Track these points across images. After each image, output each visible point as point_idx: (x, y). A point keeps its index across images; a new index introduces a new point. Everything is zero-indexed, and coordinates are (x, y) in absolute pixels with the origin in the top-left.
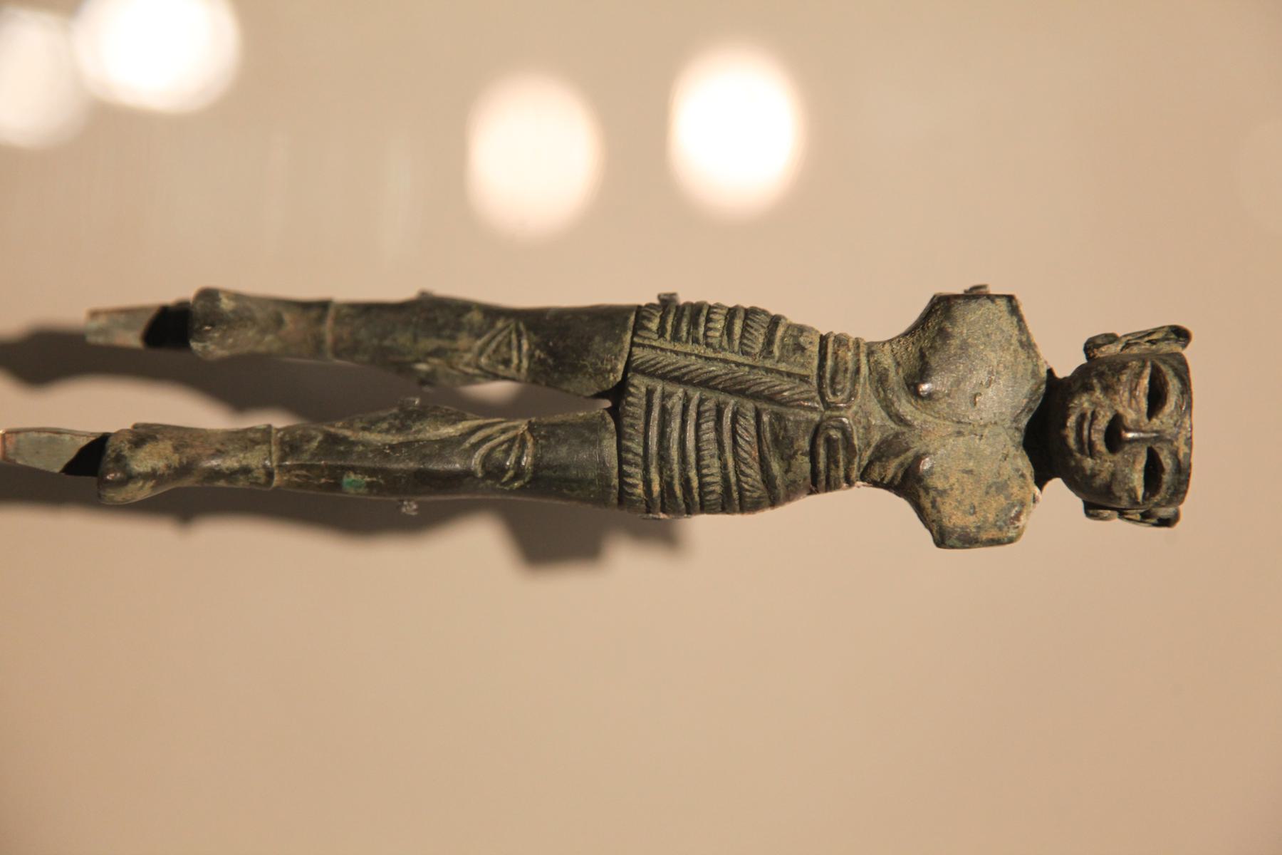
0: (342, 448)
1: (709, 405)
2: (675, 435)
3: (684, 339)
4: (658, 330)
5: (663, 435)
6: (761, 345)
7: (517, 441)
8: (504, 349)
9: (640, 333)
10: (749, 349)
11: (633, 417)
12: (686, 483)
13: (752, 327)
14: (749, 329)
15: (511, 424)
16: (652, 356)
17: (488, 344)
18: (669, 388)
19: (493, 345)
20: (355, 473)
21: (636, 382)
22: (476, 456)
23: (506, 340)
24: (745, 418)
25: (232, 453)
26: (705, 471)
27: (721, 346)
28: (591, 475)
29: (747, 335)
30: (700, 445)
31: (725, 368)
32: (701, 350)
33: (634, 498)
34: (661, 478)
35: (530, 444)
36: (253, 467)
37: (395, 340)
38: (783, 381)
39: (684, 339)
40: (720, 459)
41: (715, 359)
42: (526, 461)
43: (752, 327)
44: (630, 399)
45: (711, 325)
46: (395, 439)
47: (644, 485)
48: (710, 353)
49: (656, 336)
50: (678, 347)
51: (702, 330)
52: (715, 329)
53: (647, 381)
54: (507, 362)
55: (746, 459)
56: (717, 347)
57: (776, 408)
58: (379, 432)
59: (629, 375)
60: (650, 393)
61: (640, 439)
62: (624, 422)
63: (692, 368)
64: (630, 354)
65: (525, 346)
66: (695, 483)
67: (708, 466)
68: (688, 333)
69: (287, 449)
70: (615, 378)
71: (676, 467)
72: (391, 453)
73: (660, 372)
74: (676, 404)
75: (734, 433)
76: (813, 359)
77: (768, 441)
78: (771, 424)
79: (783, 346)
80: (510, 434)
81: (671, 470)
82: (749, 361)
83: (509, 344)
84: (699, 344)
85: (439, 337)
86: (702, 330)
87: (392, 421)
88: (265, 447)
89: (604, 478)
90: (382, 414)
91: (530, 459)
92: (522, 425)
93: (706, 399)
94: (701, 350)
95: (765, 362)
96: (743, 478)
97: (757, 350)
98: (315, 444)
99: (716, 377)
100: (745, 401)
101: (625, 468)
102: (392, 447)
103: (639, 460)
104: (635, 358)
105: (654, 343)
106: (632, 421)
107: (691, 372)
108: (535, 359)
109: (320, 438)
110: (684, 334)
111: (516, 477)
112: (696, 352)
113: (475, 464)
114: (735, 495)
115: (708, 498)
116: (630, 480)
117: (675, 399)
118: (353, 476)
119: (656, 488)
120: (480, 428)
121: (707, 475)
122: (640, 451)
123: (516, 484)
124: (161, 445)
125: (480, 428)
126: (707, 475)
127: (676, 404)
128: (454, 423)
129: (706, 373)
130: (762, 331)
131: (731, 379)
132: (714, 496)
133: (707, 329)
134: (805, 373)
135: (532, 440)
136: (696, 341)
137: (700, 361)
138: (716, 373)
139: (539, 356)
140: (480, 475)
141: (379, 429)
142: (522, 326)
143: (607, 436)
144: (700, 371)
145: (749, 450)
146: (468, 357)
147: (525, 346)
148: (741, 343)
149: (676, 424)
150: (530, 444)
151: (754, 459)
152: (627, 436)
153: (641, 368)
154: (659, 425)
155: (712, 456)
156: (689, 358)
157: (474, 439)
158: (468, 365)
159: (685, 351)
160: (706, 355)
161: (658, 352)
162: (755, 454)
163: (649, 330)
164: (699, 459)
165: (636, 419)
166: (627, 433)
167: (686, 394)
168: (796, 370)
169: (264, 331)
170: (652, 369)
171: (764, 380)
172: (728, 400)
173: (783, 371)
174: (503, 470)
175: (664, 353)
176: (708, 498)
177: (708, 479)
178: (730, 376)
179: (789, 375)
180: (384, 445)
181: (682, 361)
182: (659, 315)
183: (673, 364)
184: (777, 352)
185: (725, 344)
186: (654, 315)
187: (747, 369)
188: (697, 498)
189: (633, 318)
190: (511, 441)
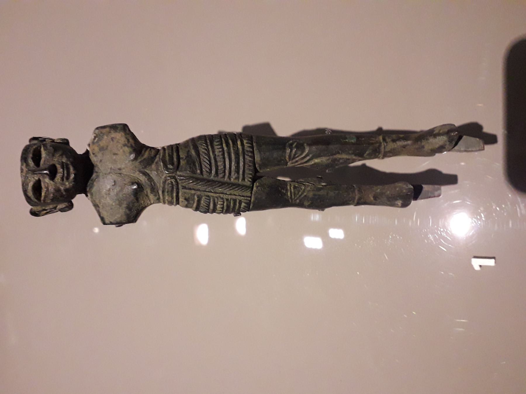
0: (357, 151)
1: (221, 176)
2: (233, 163)
3: (232, 200)
4: (242, 203)
5: (238, 163)
6: (202, 199)
7: (292, 158)
8: (296, 192)
9: (248, 201)
10: (207, 198)
11: (249, 170)
12: (228, 145)
13: (206, 206)
14: (207, 205)
15: (293, 165)
16: (244, 193)
17: (302, 194)
18: (236, 181)
19: (300, 193)
20: (352, 142)
21: (249, 183)
22: (307, 151)
23: (296, 195)
24: (207, 171)
25: (399, 147)
26: (221, 150)
27: (218, 199)
28: (264, 146)
29: (208, 203)
30: (223, 160)
31: (216, 190)
32: (225, 197)
33: (247, 139)
34: (237, 147)
35: (287, 157)
36: (391, 142)
37: (334, 193)
38: (192, 186)
39: (232, 200)
40: (215, 155)
41: (219, 193)
42: (288, 151)
43: (206, 206)
44: (251, 176)
45: (222, 206)
46: (338, 156)
47: (244, 143)
48: (222, 195)
49: (242, 200)
50: (234, 197)
51: (225, 204)
52: (219, 204)
53: (245, 183)
54: (295, 187)
55: (205, 155)
56: (219, 198)
57: (195, 176)
58: (343, 158)
59: (251, 185)
60: (244, 179)
61: (247, 161)
62: (253, 167)
63: (228, 190)
64: (251, 193)
65: (289, 193)
66: (224, 145)
67: (220, 152)
68: (230, 203)
69: (378, 150)
70: (256, 184)
71: (232, 151)
72: (339, 150)
73: (240, 187)
74: (234, 175)
75: (210, 165)
76: (181, 195)
77: (197, 162)
78: (196, 169)
79: (193, 200)
80: (294, 161)
81: (234, 150)
82: (206, 193)
83: (295, 194)
84: (226, 199)
85: (319, 195)
86: (225, 204)
87: (338, 163)
88: (387, 150)
89: (259, 145)
90: (342, 166)
91: (287, 152)
92: (290, 164)
93: (222, 178)
94: (225, 197)
95: (200, 194)
96: (206, 148)
97: (204, 198)
98: (367, 152)
99: (219, 186)
100: (207, 178)
101: (251, 150)
102: (339, 153)
103: (246, 153)
104: (249, 192)
105: (243, 198)
106: (249, 168)
107: (228, 188)
108: (285, 189)
109: (365, 155)
110: (232, 202)
111: (291, 145)
112: (227, 196)
113: (307, 148)
114: (208, 141)
115: (219, 140)
116: (249, 145)
117: (234, 177)
118: (353, 141)
119: (239, 143)
120: (306, 162)
121: (220, 148)
122: (246, 157)
123: (291, 142)
124: (430, 148)
125: (306, 162)
126: (220, 148)
127: (234, 175)
128: (315, 164)
129: (223, 188)
130: (202, 205)
131: (213, 186)
132: (216, 140)
133: (223, 204)
134: (184, 190)
135: (286, 159)
136: (227, 200)
137: (225, 192)
138: (219, 188)
139: (284, 190)
140: (305, 144)
141: (343, 160)
142: (290, 200)
143: (259, 162)
144: (225, 188)
145: (204, 158)
146: (309, 189)
147: (289, 193)
148: (210, 200)
149: (233, 168)
150: (287, 157)
151: (202, 155)
152: (251, 162)
153: (248, 188)
154: (240, 166)
155: (218, 156)
156: (229, 193)
157: (308, 158)
158: (308, 186)
159: (231, 196)
160: (223, 194)
161: (241, 195)
162: (201, 157)
163: (245, 203)
164: (223, 154)
165: (248, 169)
166: (252, 163)
167: (230, 179)
168: (187, 191)
169: (382, 194)
170: (243, 188)
171: (200, 186)
172: (213, 178)
173: (192, 190)
174: (297, 147)
175: (239, 194)
176: (219, 140)
177: (219, 147)
178: (214, 187)
179: (190, 189)
180: (341, 154)
181: (232, 192)
182: (241, 209)
183: (235, 191)
184: (196, 197)
185: (216, 199)
186: (244, 209)
187: (207, 190)
188: (223, 139)
189: (251, 207)
190: (294, 158)
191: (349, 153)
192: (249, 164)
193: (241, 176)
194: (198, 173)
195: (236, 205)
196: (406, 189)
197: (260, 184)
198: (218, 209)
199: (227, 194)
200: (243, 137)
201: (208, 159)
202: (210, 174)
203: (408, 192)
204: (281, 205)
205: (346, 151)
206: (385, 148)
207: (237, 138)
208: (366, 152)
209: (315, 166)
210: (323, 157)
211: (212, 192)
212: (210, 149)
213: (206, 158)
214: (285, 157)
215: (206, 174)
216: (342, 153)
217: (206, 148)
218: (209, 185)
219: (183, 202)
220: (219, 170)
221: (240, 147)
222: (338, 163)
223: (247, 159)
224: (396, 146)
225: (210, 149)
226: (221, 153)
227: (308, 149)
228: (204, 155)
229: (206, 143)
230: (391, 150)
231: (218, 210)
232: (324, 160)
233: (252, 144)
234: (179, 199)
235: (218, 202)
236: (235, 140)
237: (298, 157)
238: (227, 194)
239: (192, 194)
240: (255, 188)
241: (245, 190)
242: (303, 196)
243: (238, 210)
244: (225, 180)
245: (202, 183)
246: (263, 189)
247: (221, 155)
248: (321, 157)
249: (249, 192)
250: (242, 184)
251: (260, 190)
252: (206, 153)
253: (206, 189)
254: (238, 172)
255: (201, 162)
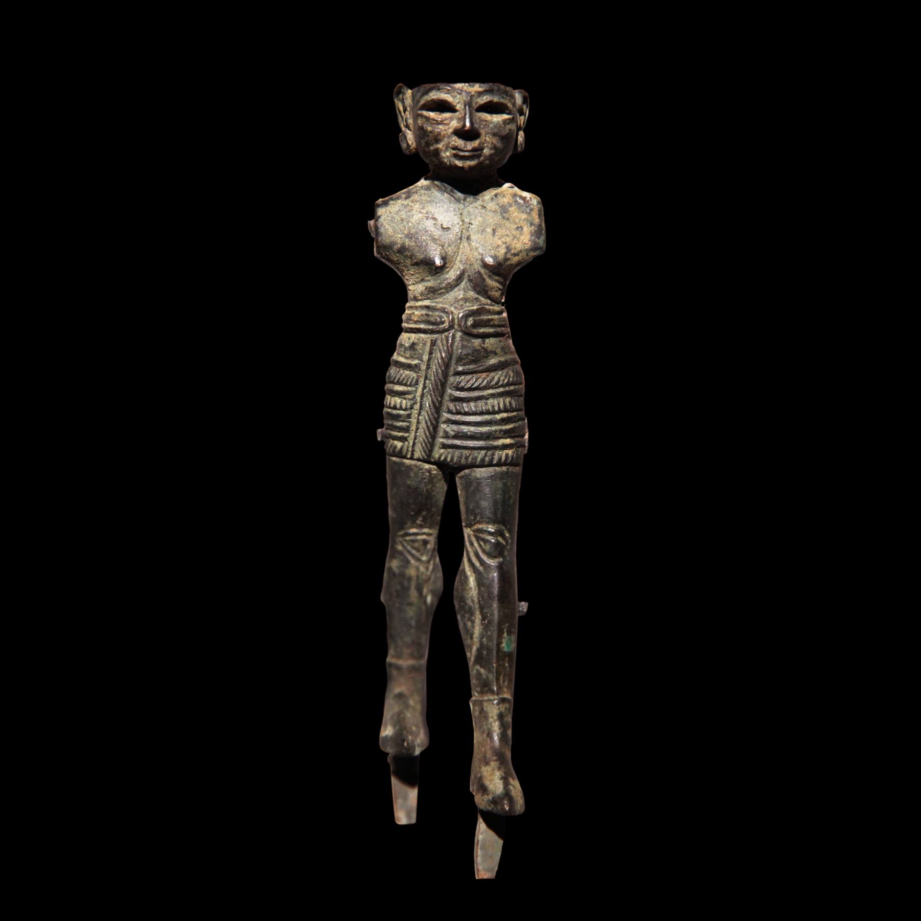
1: (452, 406)
2: (472, 429)
3: (408, 424)
4: (402, 442)
5: (473, 437)
6: (411, 373)
7: (478, 535)
8: (416, 545)
9: (404, 454)
10: (414, 380)
11: (461, 457)
12: (504, 421)
13: (399, 378)
14: (400, 381)
16: (420, 445)
17: (413, 556)
18: (441, 433)
19: (414, 552)
20: (501, 643)
21: (437, 456)
22: (489, 562)
23: (411, 543)
24: (460, 383)
25: (489, 726)
26: (496, 408)
27: (412, 399)
28: (500, 485)
30: (478, 412)
31: (427, 396)
32: (415, 412)
33: (515, 456)
34: (501, 438)
35: (480, 526)
36: (498, 711)
37: (411, 618)
38: (435, 357)
39: (408, 424)
40: (488, 399)
41: (421, 403)
42: (491, 529)
43: (399, 378)
44: (449, 459)
45: (398, 406)
46: (478, 617)
47: (506, 450)
48: (417, 406)
49: (406, 443)
50: (413, 427)
51: (402, 412)
52: (401, 403)
53: (436, 449)
54: (425, 542)
55: (488, 381)
56: (413, 402)
57: (453, 362)
58: (473, 627)
59: (433, 460)
60: (444, 446)
61: (475, 453)
62: (464, 463)
63: (427, 418)
64: (419, 460)
65: (414, 530)
66: (505, 415)
67: (493, 407)
68: (404, 421)
69: (486, 689)
70: (435, 470)
71: (494, 428)
72: (488, 619)
73: (430, 440)
74: (451, 429)
75: (470, 389)
76: (420, 337)
77: (476, 366)
78: (464, 365)
79: (412, 357)
80: (473, 539)
81: (496, 431)
82: (422, 380)
83: (413, 541)
84: (411, 414)
85: (409, 588)
86: (402, 412)
87: (466, 619)
88: (485, 704)
91: (490, 526)
93: (448, 408)
94: (415, 412)
95: (422, 369)
96: (501, 383)
98: (482, 671)
99: (433, 402)
100: (449, 382)
101: (495, 462)
102: (483, 619)
103: (489, 453)
104: (421, 457)
105: (411, 444)
106: (464, 458)
107: (430, 419)
108: (423, 523)
110: (404, 424)
111: (503, 536)
112: (416, 416)
113: (494, 562)
114: (512, 388)
115: (514, 406)
116: (503, 458)
117: (448, 429)
118: (504, 645)
119: (508, 441)
120: (470, 560)
121: (499, 407)
122: (483, 452)
123: (507, 535)
124: (485, 774)
125: (470, 560)
126: (499, 407)
127: (451, 429)
128: (466, 578)
129: (430, 409)
130: (402, 371)
131: (434, 392)
132: (513, 402)
133: (401, 408)
134: (430, 342)
135: (477, 525)
136: (409, 416)
137: (422, 413)
138: (431, 402)
139: (421, 521)
140: (501, 559)
141: (472, 628)
142: (401, 533)
143: (474, 474)
144: (429, 413)
145: (481, 379)
146: (422, 569)
147: (414, 530)
148: (410, 386)
149: (465, 428)
150: (480, 526)
151: (488, 376)
152: (474, 461)
153: (428, 453)
154: (466, 440)
155: (486, 404)
156: (421, 421)
157: (477, 564)
158: (427, 569)
159: (416, 423)
160: (418, 409)
161: (416, 441)
162: (484, 375)
163: (402, 447)
164: (488, 413)
165: (462, 455)
166: (471, 461)
167: (444, 422)
168: (428, 348)
169: (407, 706)
170: (429, 445)
171: (435, 370)
172: (449, 393)
173: (429, 357)
174: (498, 544)
175: (418, 437)
176: (514, 406)
177: (502, 406)
178: (432, 393)
179: (431, 353)
180: (482, 624)
181: (423, 425)
182: (392, 441)
183: (425, 431)
184: (416, 362)
185: (410, 396)
186: (392, 445)
187: (427, 381)
188: (515, 414)
190: (478, 538)
191: (482, 638)
192: (471, 457)
193: (450, 442)
194: (457, 368)
195: (399, 432)
196: (413, 741)
197: (433, 476)
198: (393, 399)
199: (419, 415)
200: (517, 449)
201: (481, 386)
202: (454, 387)
203: (408, 744)
204: (395, 516)
205: (487, 632)
206: (489, 700)
207: (517, 439)
208: (484, 669)
209: (463, 578)
210: (477, 591)
211: (423, 390)
212: (498, 390)
213: (483, 382)
214: (480, 522)
215: (455, 381)
216: (484, 626)
217: (501, 383)
218: (437, 385)
219: (407, 339)
220: (462, 403)
221: (501, 442)
222: (466, 619)
223: (479, 453)
224: (491, 720)
225: (498, 390)
226: (491, 409)
227: (493, 564)
228: (488, 379)
229: (508, 384)
230: (486, 713)
231: (391, 399)
232: (472, 593)
233: (505, 464)
234: (415, 333)
235: (405, 399)
236: (513, 435)
237: (480, 546)
238: (419, 415)
239: (422, 355)
240: (427, 466)
241: (426, 448)
242: (410, 558)
243: (390, 434)
244: (445, 414)
245: (441, 373)
246: (426, 482)
247: (487, 408)
248: (477, 588)
249: (421, 457)
250: (435, 442)
251: (424, 477)
252: (490, 382)
253: (430, 380)
254: (457, 436)
255: (477, 373)
